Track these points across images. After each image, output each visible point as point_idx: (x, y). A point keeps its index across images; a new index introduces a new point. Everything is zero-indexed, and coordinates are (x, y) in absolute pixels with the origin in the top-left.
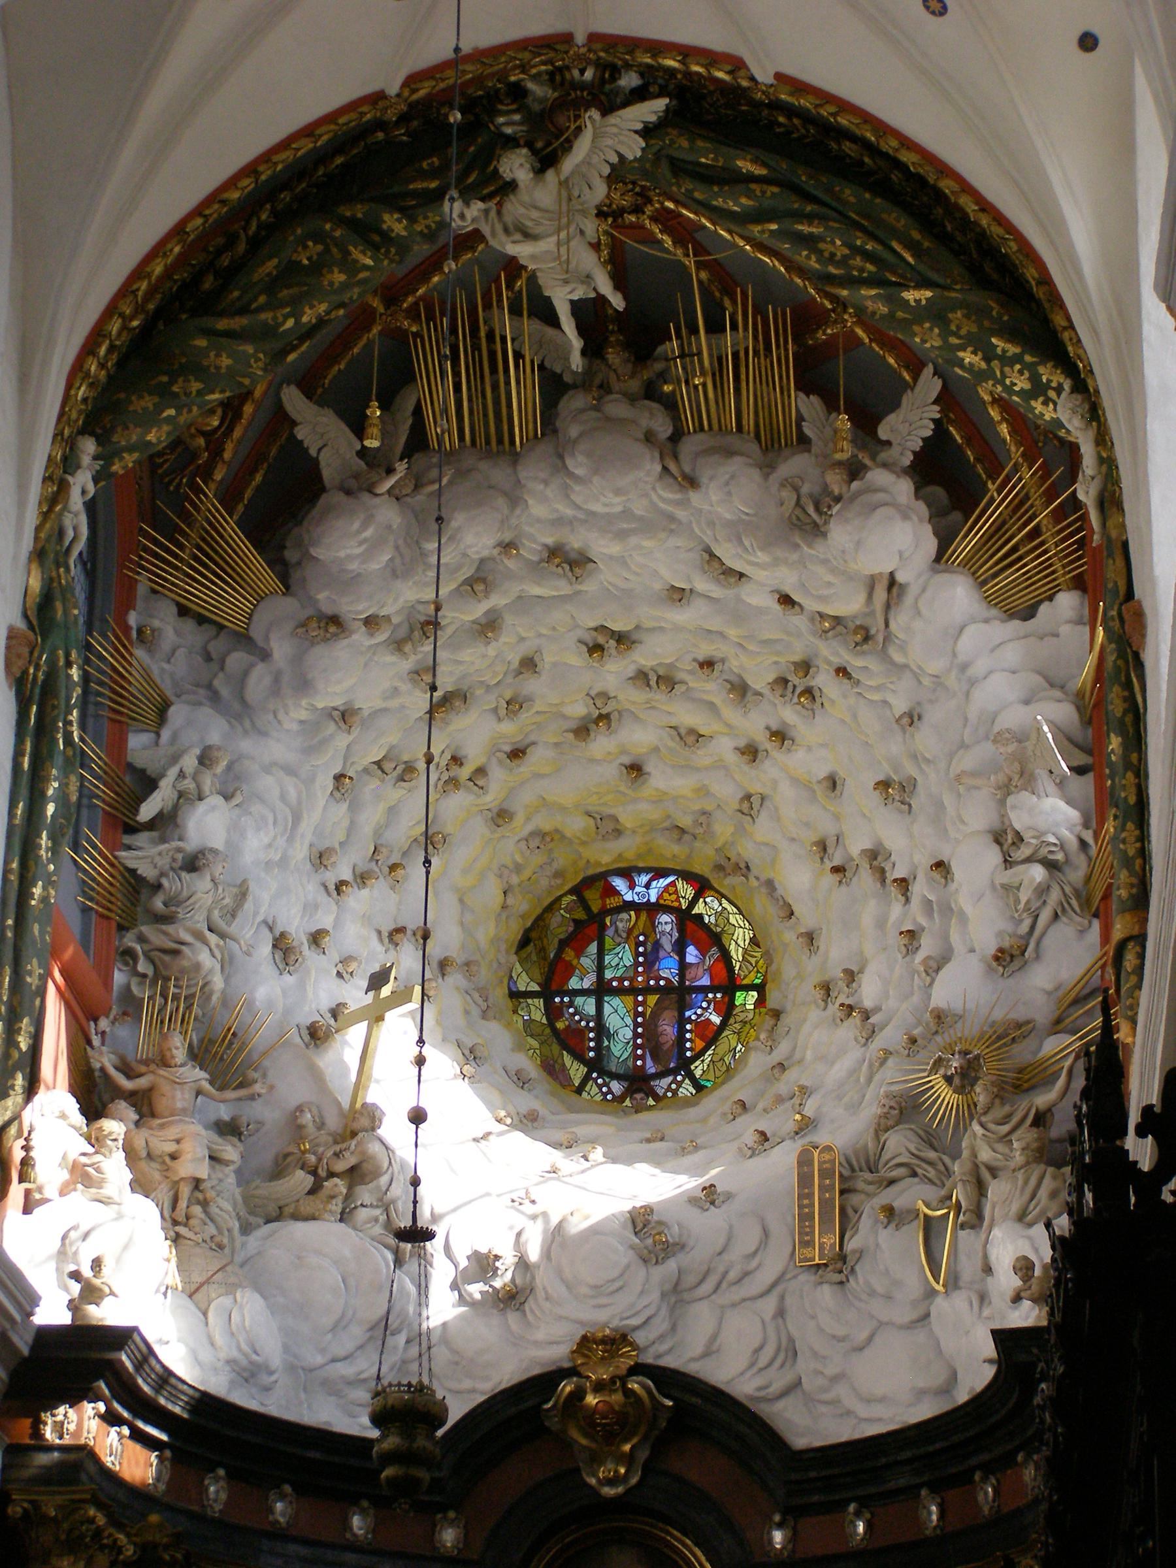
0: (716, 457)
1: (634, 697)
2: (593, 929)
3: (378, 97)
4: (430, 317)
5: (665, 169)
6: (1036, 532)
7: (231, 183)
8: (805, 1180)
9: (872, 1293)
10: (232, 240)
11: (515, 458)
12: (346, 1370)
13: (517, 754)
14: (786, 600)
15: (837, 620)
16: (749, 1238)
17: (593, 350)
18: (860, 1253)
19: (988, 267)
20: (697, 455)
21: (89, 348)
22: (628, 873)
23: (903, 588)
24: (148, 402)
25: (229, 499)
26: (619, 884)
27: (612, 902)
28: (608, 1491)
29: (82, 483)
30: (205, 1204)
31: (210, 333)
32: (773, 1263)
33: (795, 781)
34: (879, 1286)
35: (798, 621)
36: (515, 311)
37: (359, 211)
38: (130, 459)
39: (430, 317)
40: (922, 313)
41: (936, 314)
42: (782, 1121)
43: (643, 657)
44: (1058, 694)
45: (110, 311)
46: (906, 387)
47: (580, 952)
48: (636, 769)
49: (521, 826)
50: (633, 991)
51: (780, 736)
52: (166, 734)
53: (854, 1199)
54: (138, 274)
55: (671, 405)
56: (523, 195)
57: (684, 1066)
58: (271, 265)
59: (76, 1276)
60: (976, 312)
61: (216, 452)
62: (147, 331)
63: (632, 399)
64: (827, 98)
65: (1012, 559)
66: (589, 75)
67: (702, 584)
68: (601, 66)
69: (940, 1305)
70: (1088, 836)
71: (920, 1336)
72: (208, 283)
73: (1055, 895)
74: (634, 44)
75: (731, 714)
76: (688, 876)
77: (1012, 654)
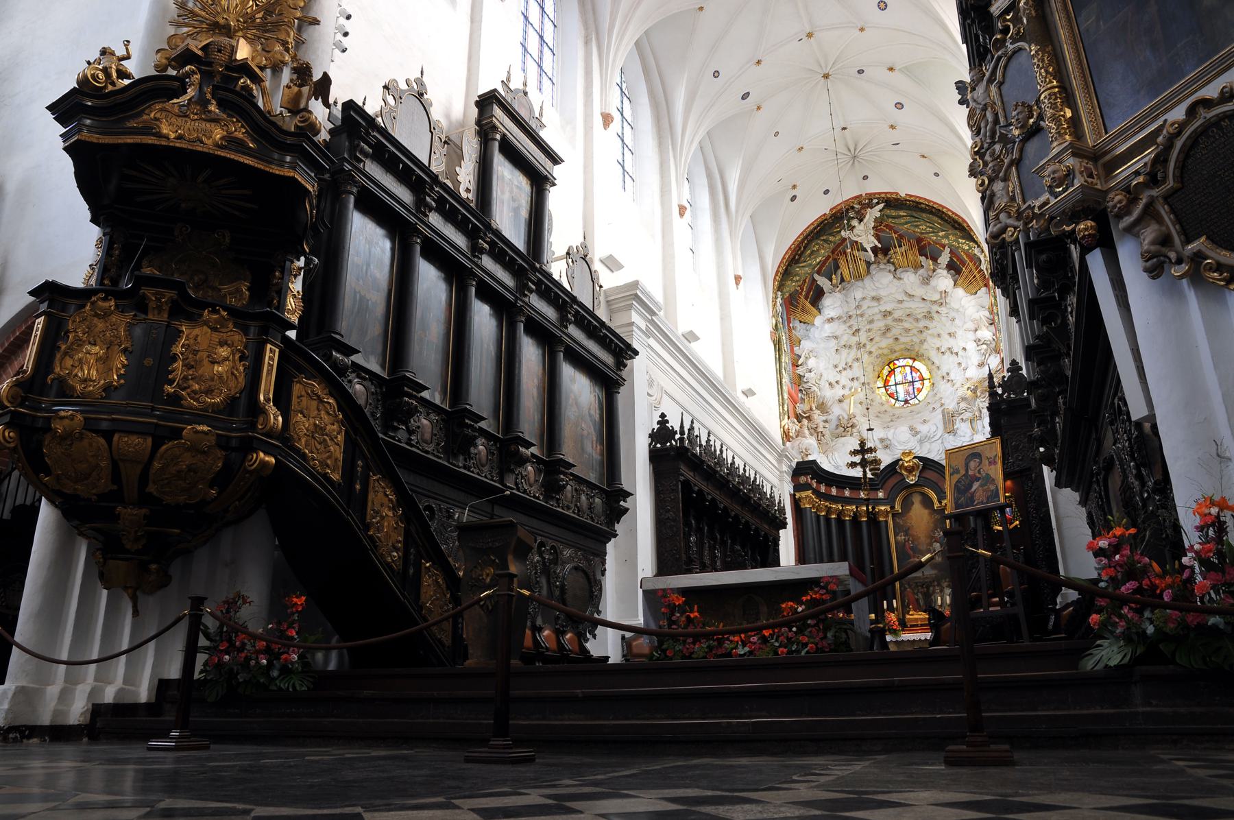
0: (904, 273)
3: (825, 214)
4: (841, 255)
5: (885, 217)
6: (975, 276)
7: (799, 237)
8: (944, 416)
10: (800, 248)
14: (924, 299)
15: (935, 302)
16: (934, 429)
17: (876, 255)
19: (956, 225)
20: (900, 273)
21: (776, 275)
22: (898, 360)
23: (948, 293)
24: (790, 282)
25: (806, 299)
27: (896, 366)
28: (911, 483)
29: (779, 300)
30: (823, 436)
32: (940, 433)
33: (930, 335)
34: (962, 434)
36: (858, 250)
37: (825, 238)
38: (787, 295)
39: (841, 255)
40: (943, 237)
41: (946, 237)
42: (937, 405)
44: (984, 309)
45: (779, 266)
46: (942, 251)
47: (890, 377)
49: (875, 354)
50: (903, 383)
54: (784, 258)
55: (893, 264)
56: (857, 228)
57: (915, 397)
59: (802, 452)
60: (956, 235)
61: (802, 289)
62: (786, 269)
63: (885, 264)
64: (917, 197)
65: (971, 283)
66: (867, 201)
67: (905, 299)
68: (869, 199)
70: (994, 337)
72: (797, 258)
73: (989, 351)
74: (875, 194)
75: (915, 324)
76: (910, 358)
77: (973, 302)
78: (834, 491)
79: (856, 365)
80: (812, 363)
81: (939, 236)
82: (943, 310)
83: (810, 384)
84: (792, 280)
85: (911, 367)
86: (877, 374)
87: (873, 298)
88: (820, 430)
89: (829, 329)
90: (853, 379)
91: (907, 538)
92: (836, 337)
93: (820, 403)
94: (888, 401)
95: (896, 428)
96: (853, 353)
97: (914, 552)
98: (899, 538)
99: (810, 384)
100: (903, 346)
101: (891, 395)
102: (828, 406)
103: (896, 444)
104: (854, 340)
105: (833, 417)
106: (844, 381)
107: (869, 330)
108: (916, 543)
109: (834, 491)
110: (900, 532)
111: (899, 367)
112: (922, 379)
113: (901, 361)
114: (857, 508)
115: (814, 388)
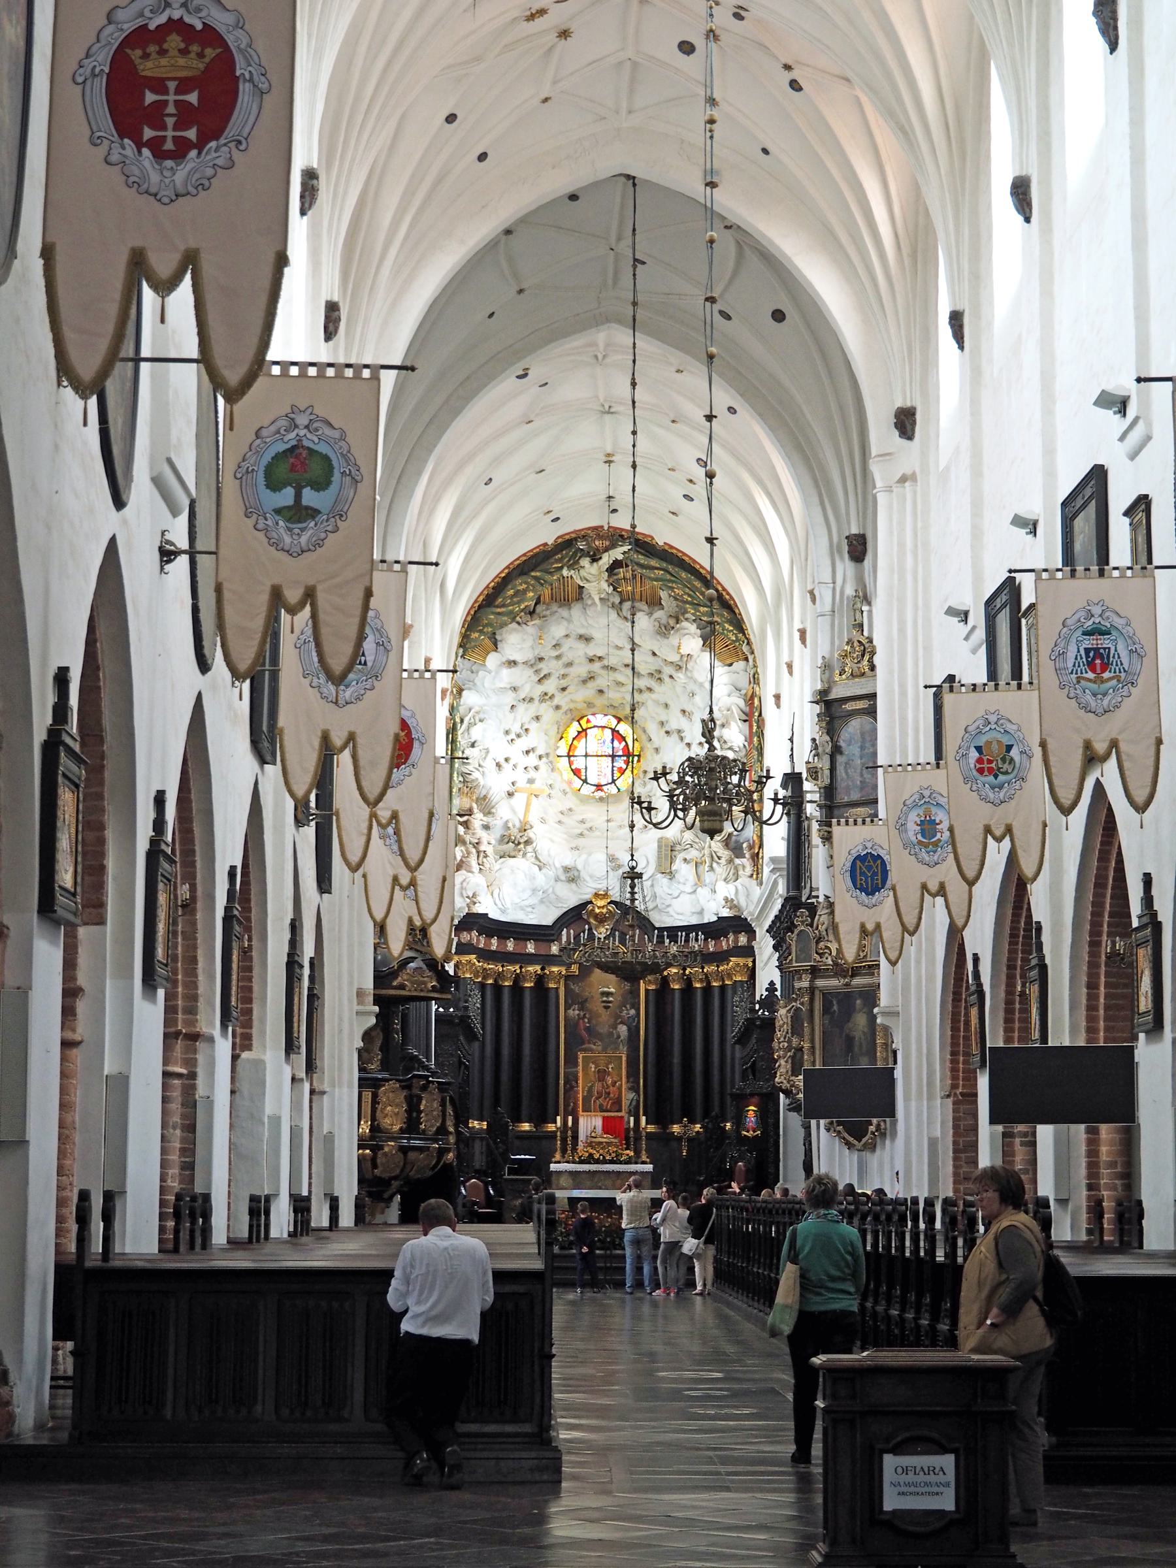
1: (604, 672)
2: (583, 734)
3: (545, 544)
8: (660, 847)
9: (679, 883)
11: (570, 609)
12: (526, 903)
13: (564, 689)
14: (654, 654)
18: (676, 871)
21: (463, 627)
24: (477, 635)
26: (590, 717)
27: (590, 725)
31: (493, 613)
33: (654, 701)
35: (659, 660)
37: (538, 574)
43: (605, 662)
47: (579, 741)
48: (601, 691)
51: (650, 689)
52: (462, 700)
53: (674, 853)
57: (614, 781)
58: (511, 592)
69: (699, 890)
70: (746, 744)
71: (693, 896)
78: (494, 941)
79: (533, 726)
80: (476, 733)
81: (700, 612)
82: (680, 676)
83: (470, 767)
84: (481, 632)
85: (613, 730)
86: (560, 736)
87: (581, 637)
88: (482, 848)
89: (507, 676)
90: (528, 752)
91: (582, 1014)
92: (515, 689)
93: (482, 796)
94: (570, 783)
95: (590, 854)
96: (533, 709)
97: (590, 1035)
98: (571, 1012)
99: (470, 767)
100: (606, 703)
101: (576, 772)
102: (493, 804)
103: (588, 879)
104: (540, 689)
105: (497, 823)
106: (517, 756)
107: (564, 676)
108: (594, 1022)
109: (494, 944)
110: (573, 1003)
111: (594, 727)
112: (628, 754)
113: (599, 716)
114: (521, 968)
115: (476, 775)
